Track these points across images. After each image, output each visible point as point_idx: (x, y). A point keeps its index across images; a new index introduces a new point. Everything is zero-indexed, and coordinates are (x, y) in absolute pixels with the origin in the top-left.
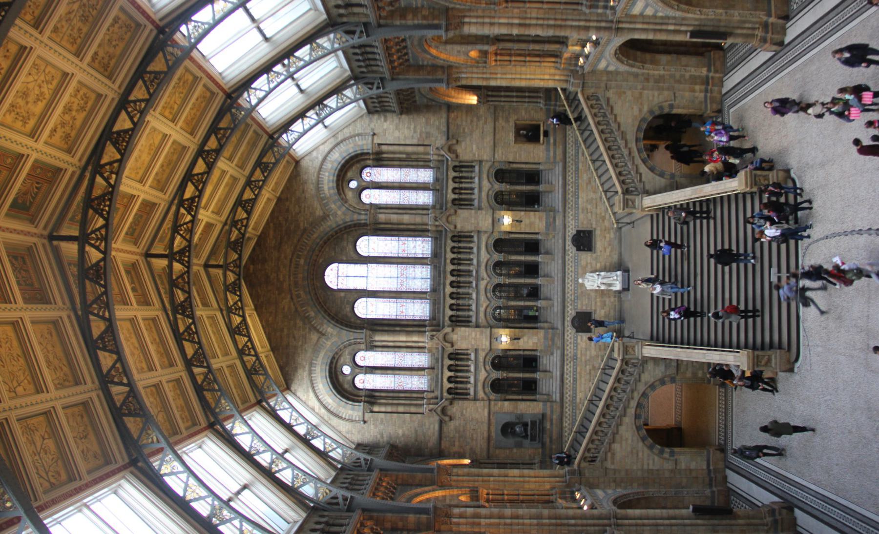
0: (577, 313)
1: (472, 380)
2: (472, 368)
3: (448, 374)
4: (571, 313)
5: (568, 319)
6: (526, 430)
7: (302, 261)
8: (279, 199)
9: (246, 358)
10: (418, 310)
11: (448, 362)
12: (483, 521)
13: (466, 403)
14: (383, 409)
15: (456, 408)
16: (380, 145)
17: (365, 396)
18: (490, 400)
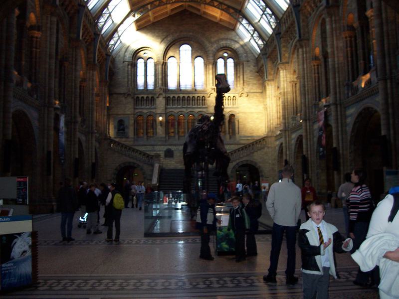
0: (173, 151)
1: (143, 107)
2: (148, 107)
3: (145, 96)
4: (173, 148)
5: (170, 147)
6: (122, 130)
7: (191, 34)
8: (217, 23)
9: (149, 6)
10: (172, 84)
11: (150, 96)
12: (91, 82)
13: (132, 105)
14: (129, 69)
15: (130, 100)
16: (243, 64)
17: (135, 63)
18: (134, 114)
